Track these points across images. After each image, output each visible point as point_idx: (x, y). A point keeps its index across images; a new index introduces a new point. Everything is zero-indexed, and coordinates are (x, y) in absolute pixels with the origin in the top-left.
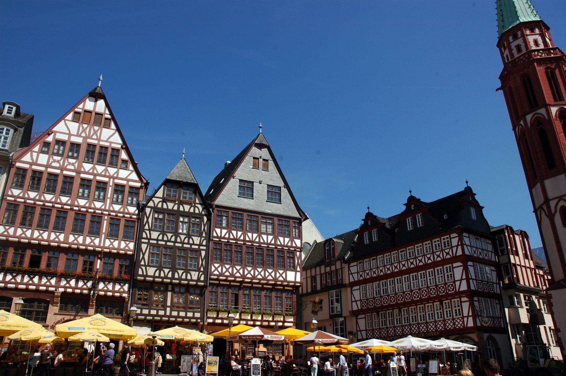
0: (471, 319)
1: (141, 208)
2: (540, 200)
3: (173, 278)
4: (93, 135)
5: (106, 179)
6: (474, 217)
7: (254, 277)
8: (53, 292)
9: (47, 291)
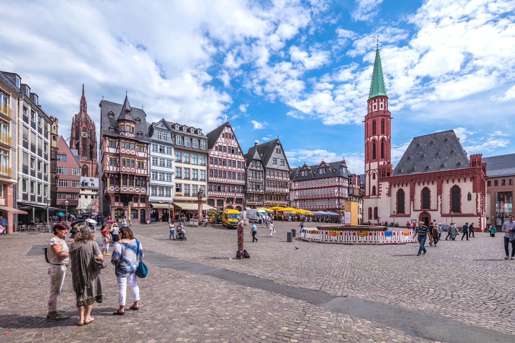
1: (246, 170)
2: (368, 169)
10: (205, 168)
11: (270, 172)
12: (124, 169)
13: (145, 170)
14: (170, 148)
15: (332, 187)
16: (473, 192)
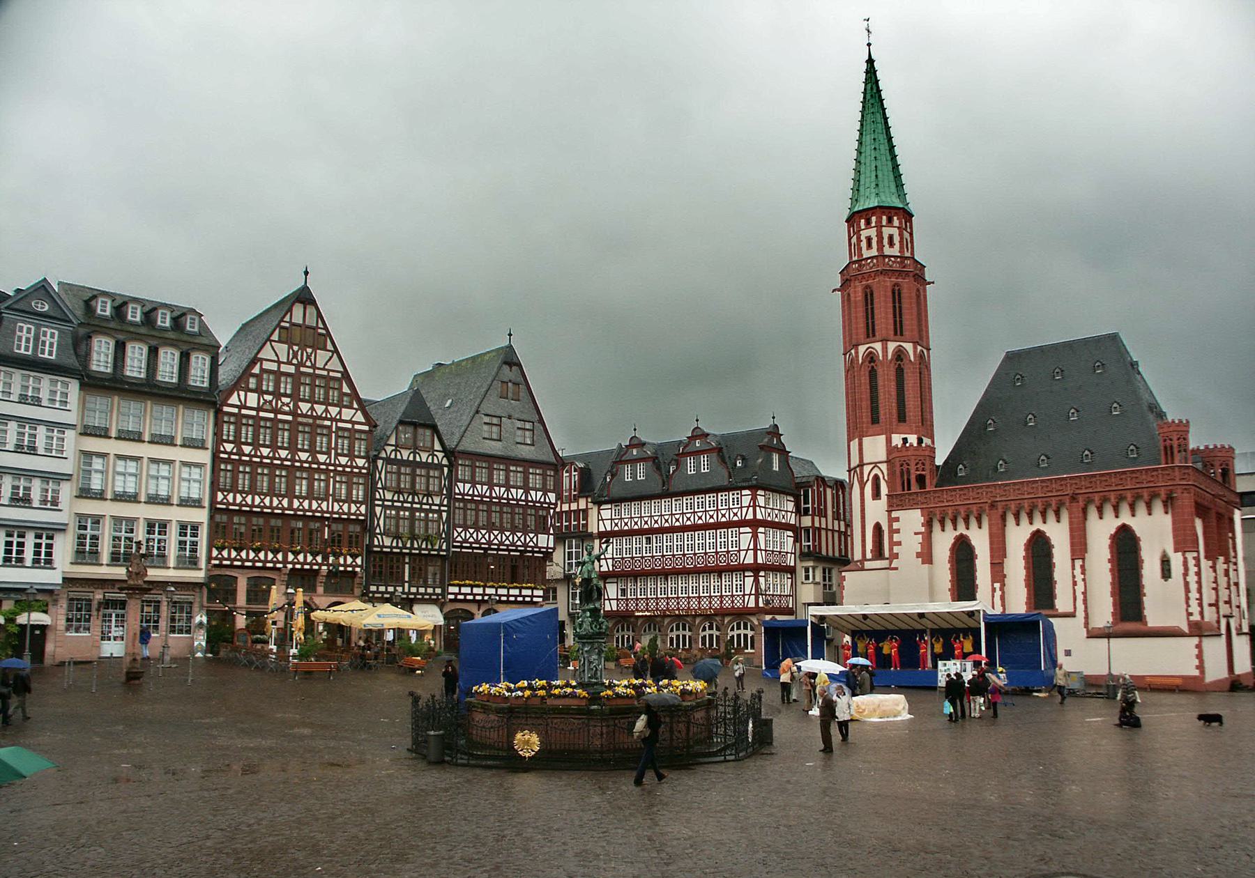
0: (753, 597)
1: (372, 460)
3: (412, 548)
5: (328, 423)
6: (776, 468)
7: (501, 543)
8: (279, 569)
9: (274, 569)
10: (205, 457)
11: (473, 467)
14: (66, 385)
15: (729, 525)
16: (1176, 551)
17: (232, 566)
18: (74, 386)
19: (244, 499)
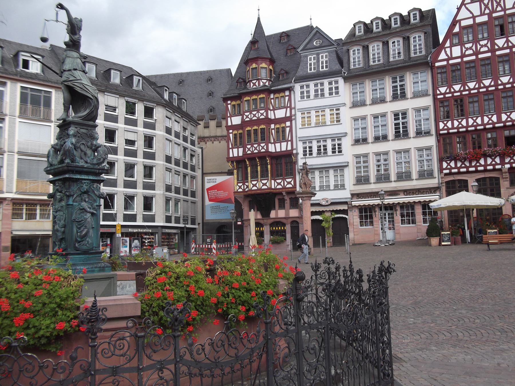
4: (497, 7)
8: (500, 170)
9: (494, 170)
10: (428, 101)
12: (249, 149)
13: (287, 141)
14: (337, 82)
17: (459, 173)
18: (341, 81)
19: (460, 123)
